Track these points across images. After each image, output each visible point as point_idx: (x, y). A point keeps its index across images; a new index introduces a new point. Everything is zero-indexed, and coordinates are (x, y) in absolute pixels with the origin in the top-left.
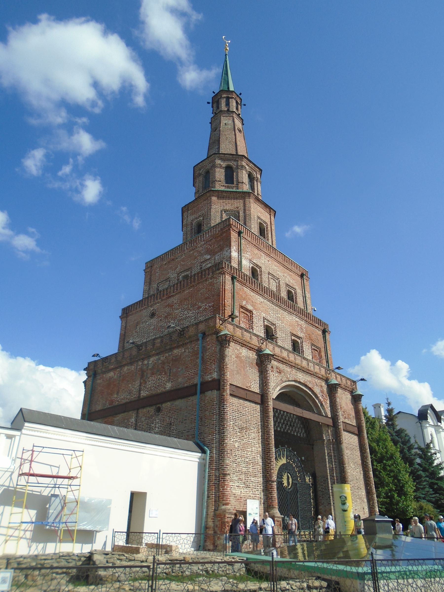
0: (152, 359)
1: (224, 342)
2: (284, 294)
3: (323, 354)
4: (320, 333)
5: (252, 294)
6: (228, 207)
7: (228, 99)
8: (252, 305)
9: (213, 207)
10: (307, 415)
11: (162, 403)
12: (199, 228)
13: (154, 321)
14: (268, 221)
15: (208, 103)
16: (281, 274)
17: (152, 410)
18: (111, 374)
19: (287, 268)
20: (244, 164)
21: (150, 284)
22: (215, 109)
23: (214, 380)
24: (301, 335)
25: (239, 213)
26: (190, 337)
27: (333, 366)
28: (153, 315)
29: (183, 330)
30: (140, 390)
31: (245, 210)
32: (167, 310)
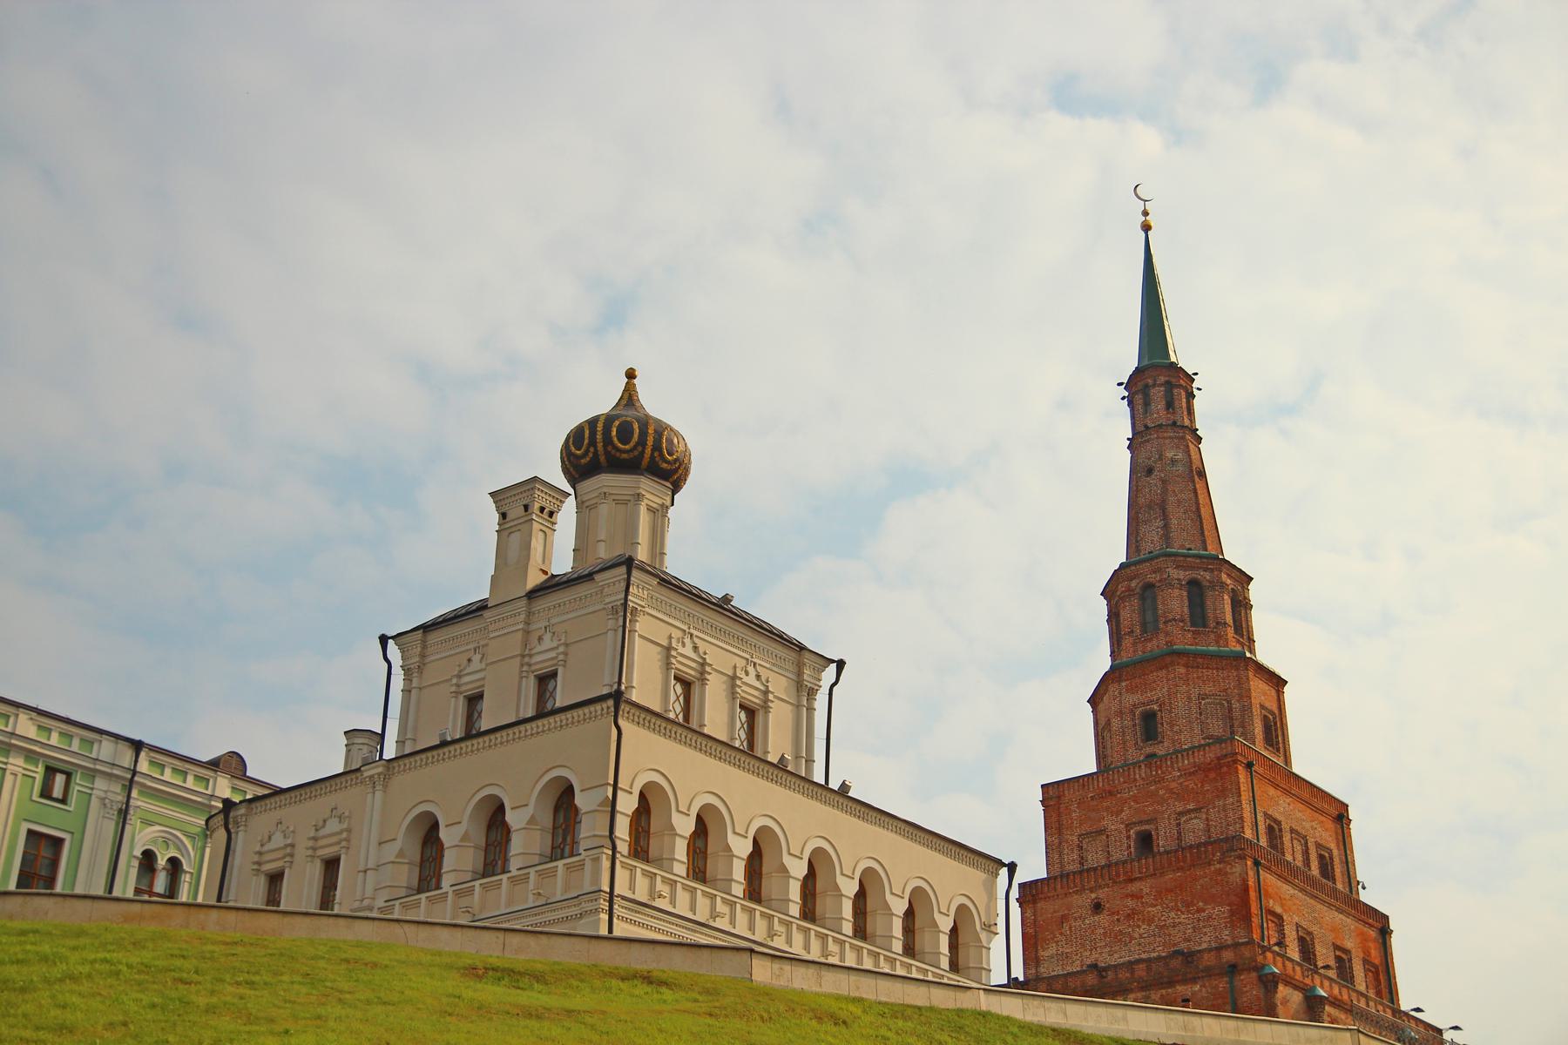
5: (1280, 883)
6: (1208, 689)
8: (1282, 906)
12: (1149, 725)
13: (1103, 919)
16: (1308, 825)
19: (1317, 810)
21: (1060, 833)
24: (1349, 944)
27: (1405, 1005)
28: (1097, 907)
32: (1130, 903)
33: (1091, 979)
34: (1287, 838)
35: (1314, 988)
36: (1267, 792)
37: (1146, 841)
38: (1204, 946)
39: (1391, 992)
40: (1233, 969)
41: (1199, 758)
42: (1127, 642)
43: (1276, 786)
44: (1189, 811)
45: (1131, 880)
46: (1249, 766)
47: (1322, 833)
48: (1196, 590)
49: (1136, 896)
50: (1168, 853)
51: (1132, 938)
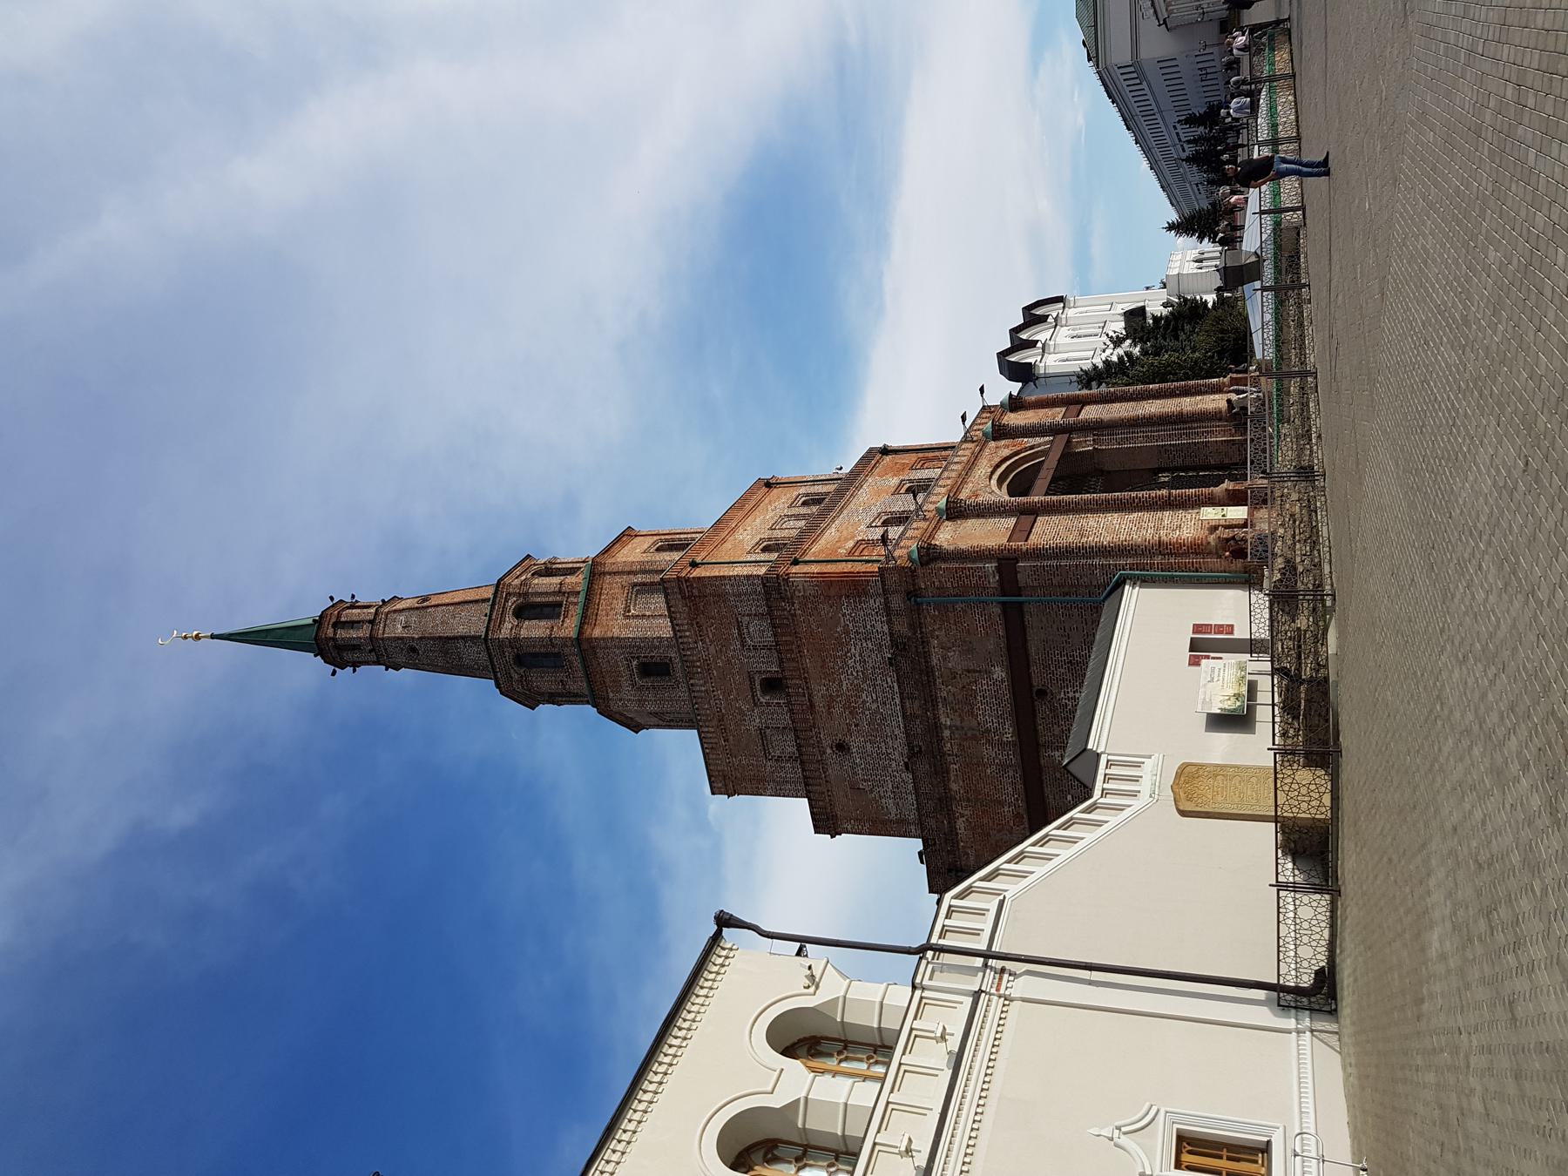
0: (945, 720)
1: (930, 554)
2: (815, 509)
3: (931, 455)
4: (888, 458)
5: (822, 542)
6: (619, 606)
7: (338, 624)
8: (847, 540)
9: (616, 632)
10: (1051, 463)
11: (1031, 686)
13: (855, 743)
14: (651, 540)
15: (334, 673)
17: (1043, 710)
18: (961, 824)
19: (757, 505)
20: (517, 582)
22: (356, 656)
23: (998, 569)
24: (895, 481)
25: (635, 585)
26: (912, 626)
27: (955, 435)
29: (894, 643)
30: (1001, 743)
31: (629, 573)
32: (837, 710)
33: (923, 767)
34: (778, 534)
35: (937, 509)
36: (726, 552)
37: (772, 685)
38: (886, 628)
39: (945, 449)
40: (912, 594)
41: (682, 620)
42: (573, 687)
43: (724, 541)
44: (740, 634)
45: (812, 706)
46: (694, 565)
47: (780, 502)
48: (527, 610)
49: (830, 701)
50: (781, 661)
51: (877, 711)
